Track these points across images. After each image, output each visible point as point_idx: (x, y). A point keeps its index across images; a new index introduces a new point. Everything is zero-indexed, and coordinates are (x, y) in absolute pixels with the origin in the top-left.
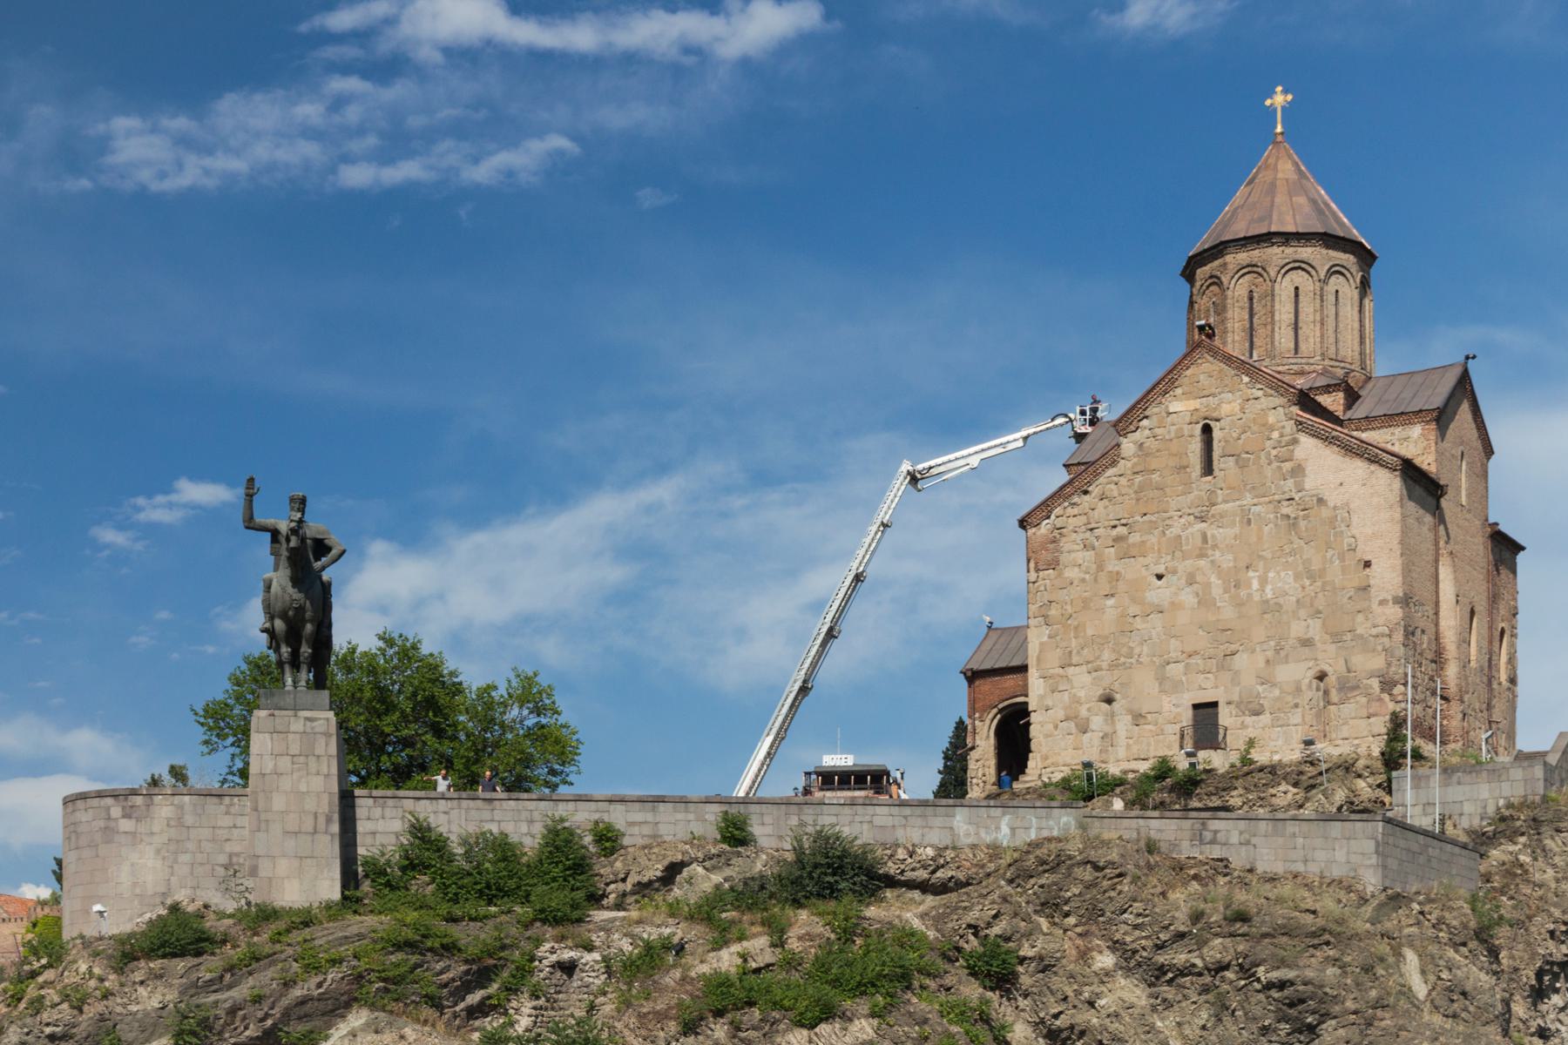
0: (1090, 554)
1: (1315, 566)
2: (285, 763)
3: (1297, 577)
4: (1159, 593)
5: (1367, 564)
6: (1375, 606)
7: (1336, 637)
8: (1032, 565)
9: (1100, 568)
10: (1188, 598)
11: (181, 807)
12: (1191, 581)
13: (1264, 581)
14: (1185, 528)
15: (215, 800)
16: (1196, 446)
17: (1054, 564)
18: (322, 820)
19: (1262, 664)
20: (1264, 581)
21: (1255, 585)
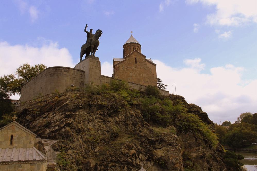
0: (123, 69)
1: (148, 74)
2: (94, 67)
3: (146, 75)
4: (131, 75)
5: (153, 75)
6: (155, 79)
7: (150, 81)
8: (116, 70)
9: (124, 71)
10: (134, 75)
11: (75, 72)
12: (135, 73)
13: (143, 75)
14: (134, 68)
15: (79, 72)
16: (135, 60)
17: (119, 70)
18: (99, 77)
19: (143, 83)
20: (143, 75)
21: (142, 75)
